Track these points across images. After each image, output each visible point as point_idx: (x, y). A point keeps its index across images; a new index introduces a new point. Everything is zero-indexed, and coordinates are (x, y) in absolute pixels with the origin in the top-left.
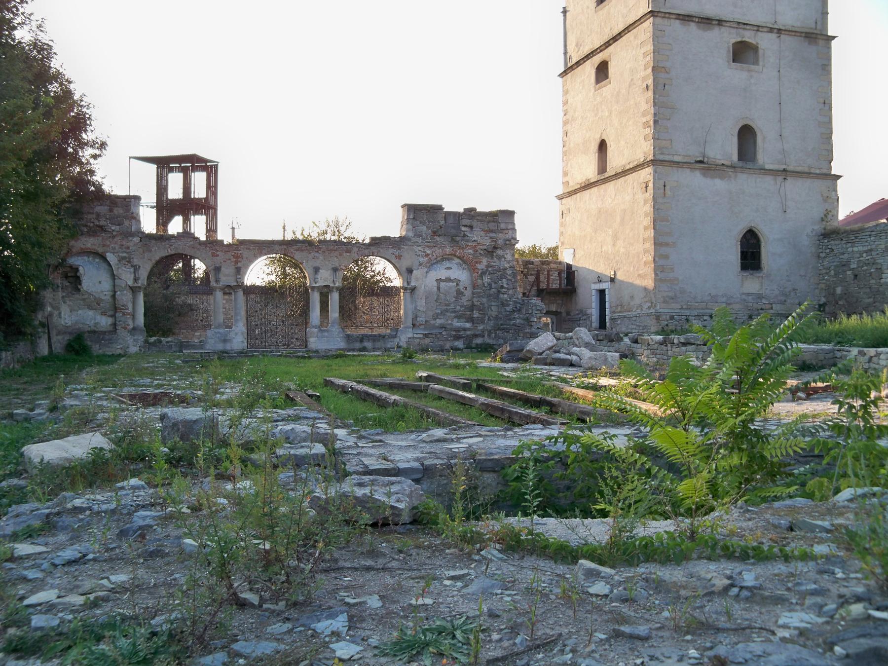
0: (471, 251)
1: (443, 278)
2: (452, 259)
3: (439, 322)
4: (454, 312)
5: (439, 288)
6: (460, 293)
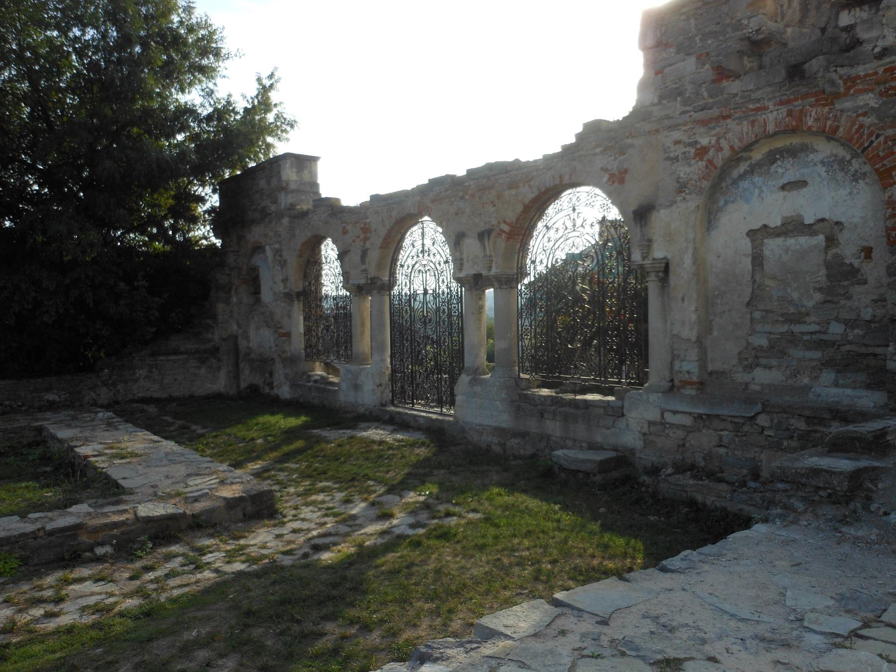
0: (870, 100)
1: (775, 221)
2: (805, 148)
3: (762, 377)
4: (821, 344)
5: (758, 260)
6: (841, 275)
